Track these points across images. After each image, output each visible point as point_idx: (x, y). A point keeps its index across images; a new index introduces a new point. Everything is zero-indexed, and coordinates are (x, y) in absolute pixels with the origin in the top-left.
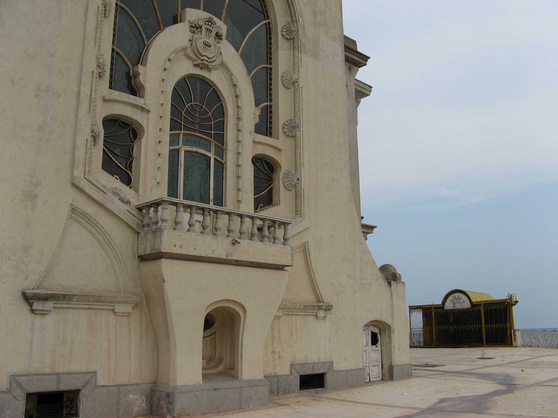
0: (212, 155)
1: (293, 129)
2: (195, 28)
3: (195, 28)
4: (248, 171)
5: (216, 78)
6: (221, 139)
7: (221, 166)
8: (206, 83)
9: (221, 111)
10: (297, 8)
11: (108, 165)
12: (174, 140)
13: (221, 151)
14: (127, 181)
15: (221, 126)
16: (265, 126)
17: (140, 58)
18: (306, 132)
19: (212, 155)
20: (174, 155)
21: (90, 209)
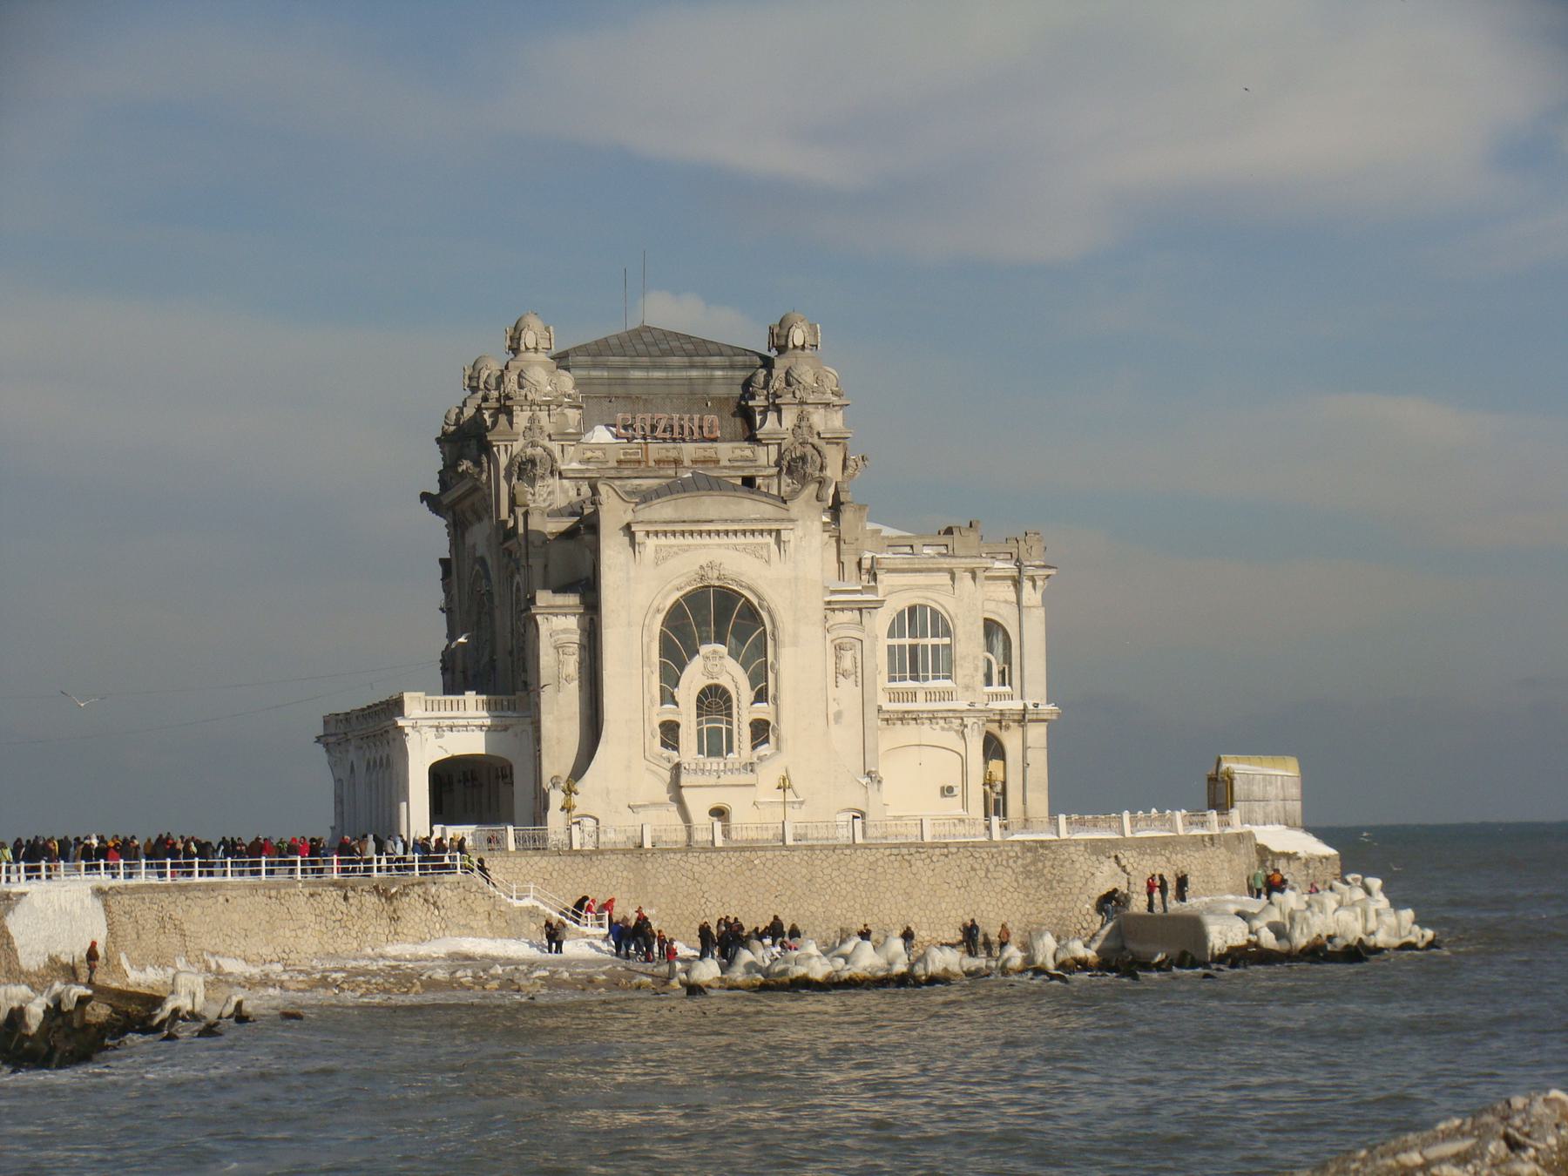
0: (724, 726)
1: (775, 698)
2: (706, 658)
3: (706, 658)
4: (746, 732)
5: (724, 681)
6: (730, 715)
7: (730, 733)
8: (717, 687)
9: (729, 699)
10: (778, 618)
11: (664, 744)
12: (699, 724)
13: (730, 723)
14: (676, 748)
15: (730, 707)
16: (761, 696)
17: (676, 685)
18: (786, 698)
19: (724, 726)
20: (700, 732)
21: (655, 768)
